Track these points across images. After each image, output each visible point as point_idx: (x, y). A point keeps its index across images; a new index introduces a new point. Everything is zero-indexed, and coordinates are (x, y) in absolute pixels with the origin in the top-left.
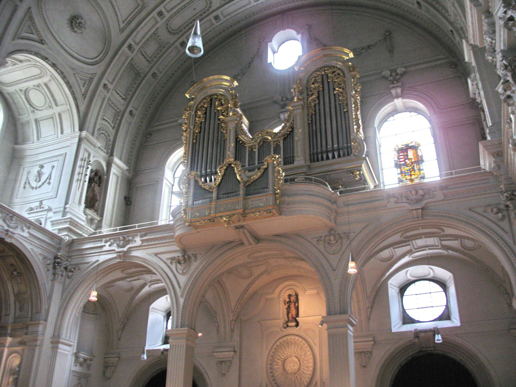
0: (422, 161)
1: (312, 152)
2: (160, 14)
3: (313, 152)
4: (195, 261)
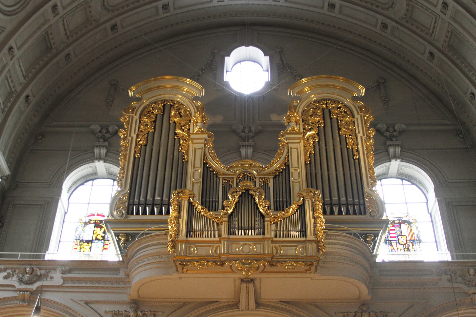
0: (420, 241)
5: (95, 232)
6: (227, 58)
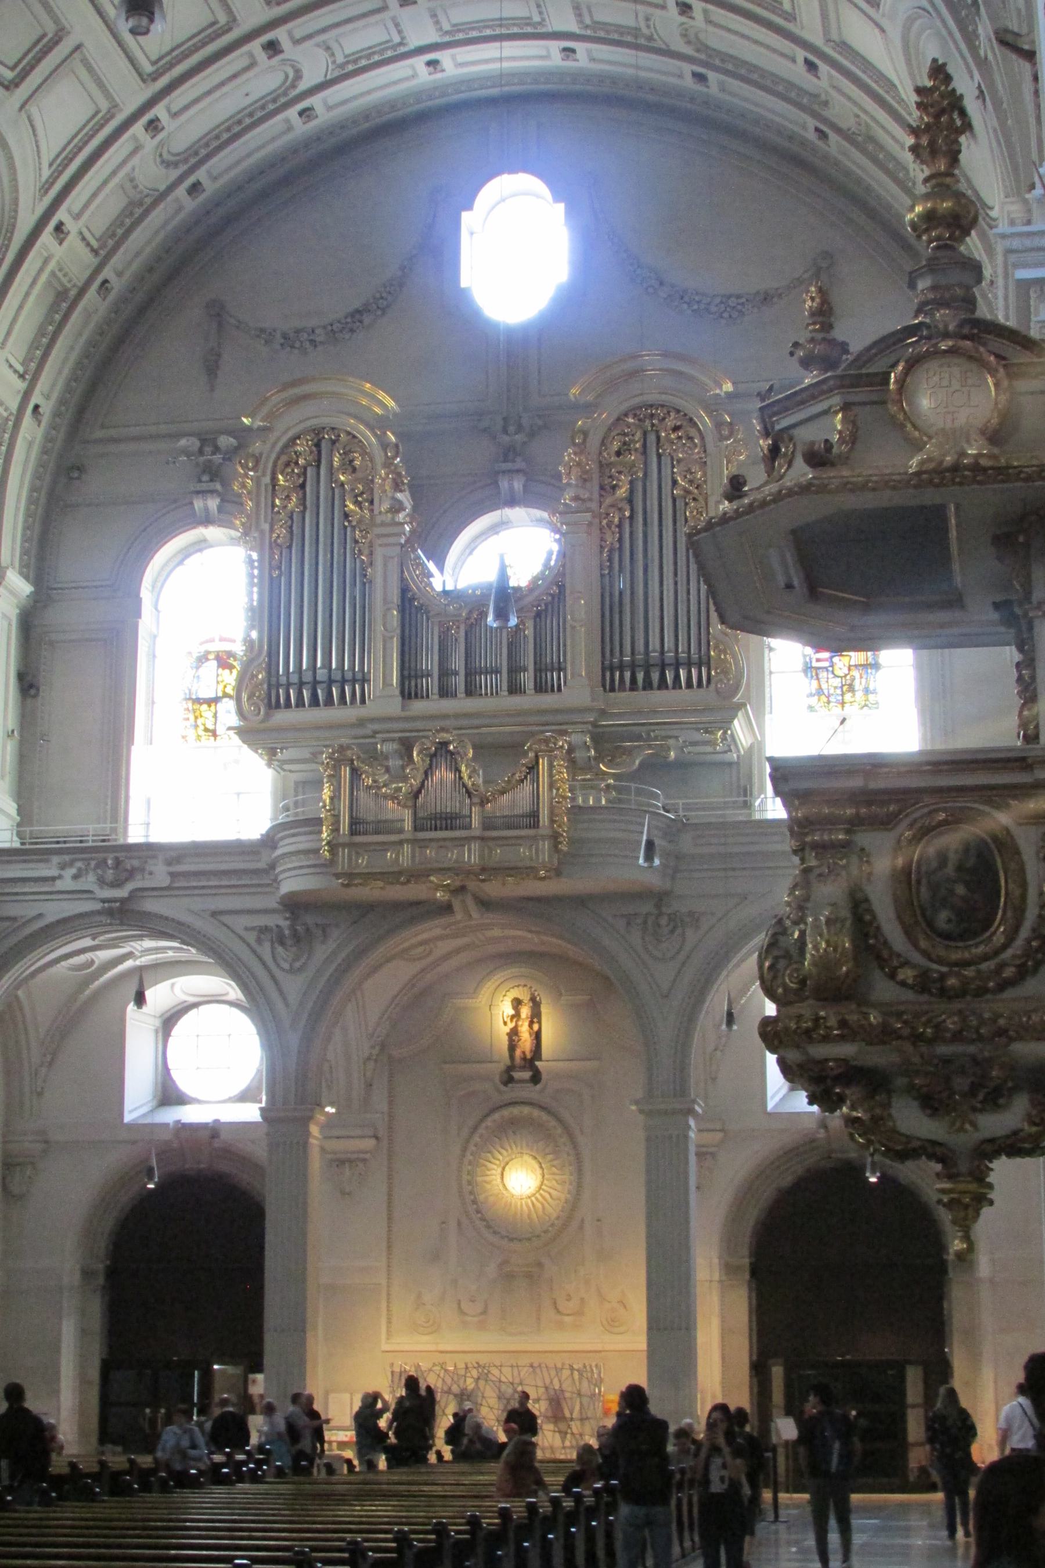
1: (607, 663)
2: (153, 126)
3: (611, 661)
4: (323, 942)
5: (220, 679)
6: (465, 216)
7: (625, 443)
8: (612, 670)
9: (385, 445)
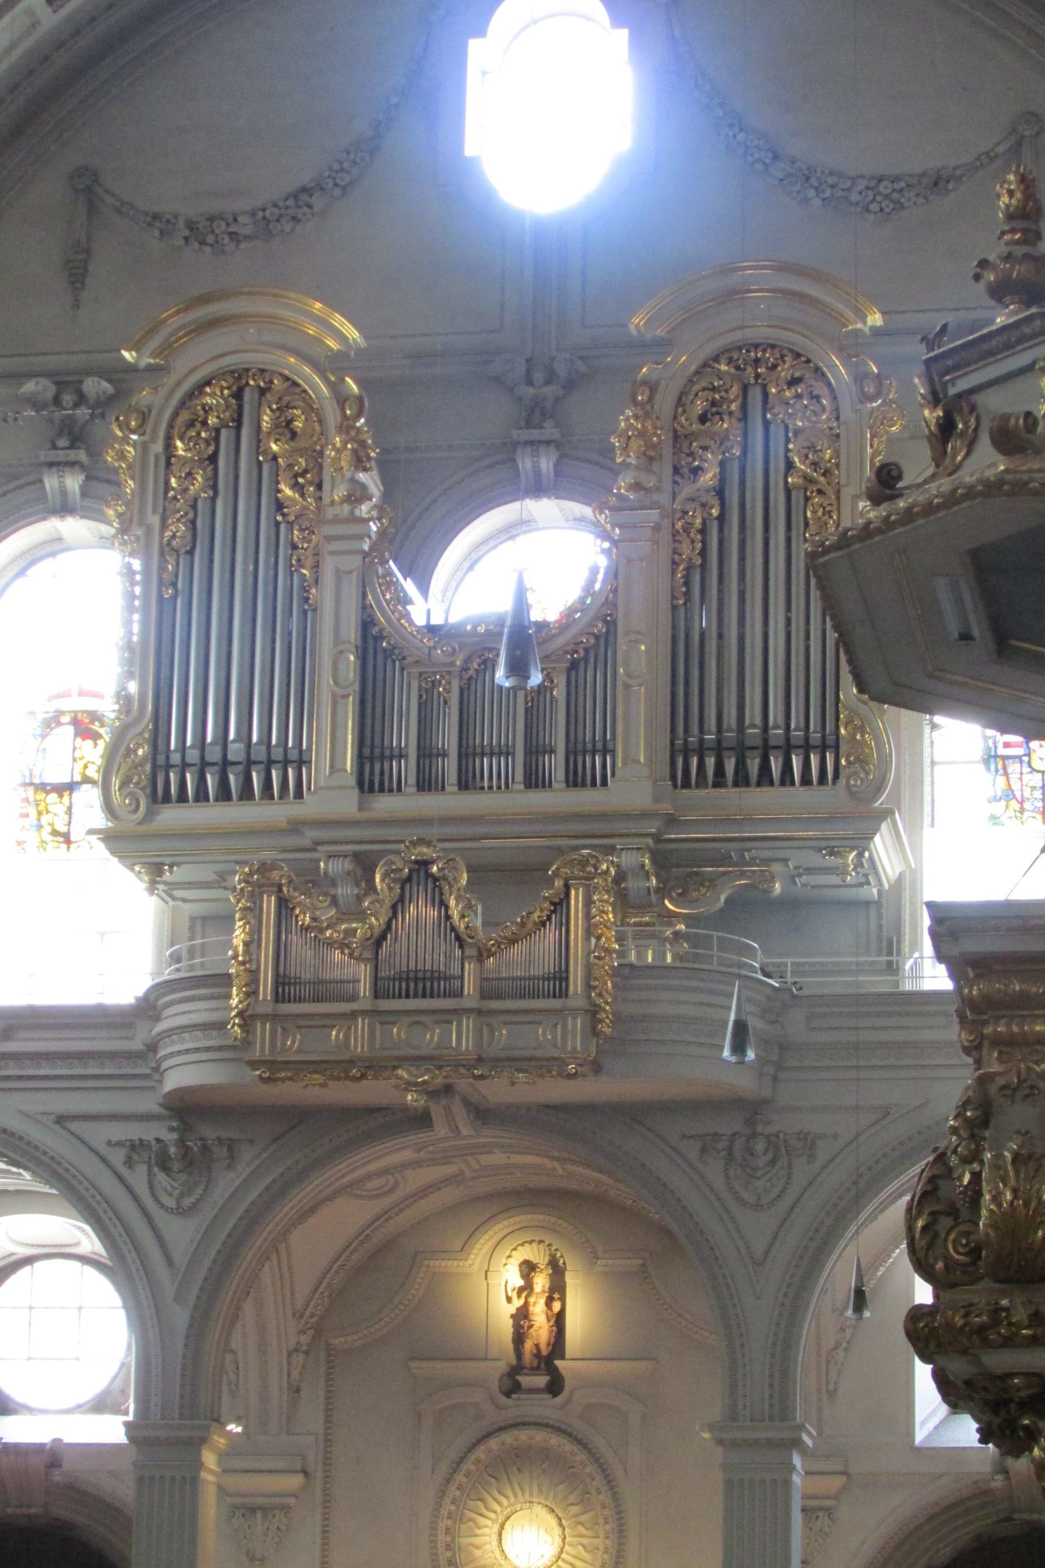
1: (679, 742)
3: (686, 741)
4: (229, 1167)
5: (78, 754)
6: (474, 45)
7: (714, 403)
8: (686, 753)
9: (341, 399)
